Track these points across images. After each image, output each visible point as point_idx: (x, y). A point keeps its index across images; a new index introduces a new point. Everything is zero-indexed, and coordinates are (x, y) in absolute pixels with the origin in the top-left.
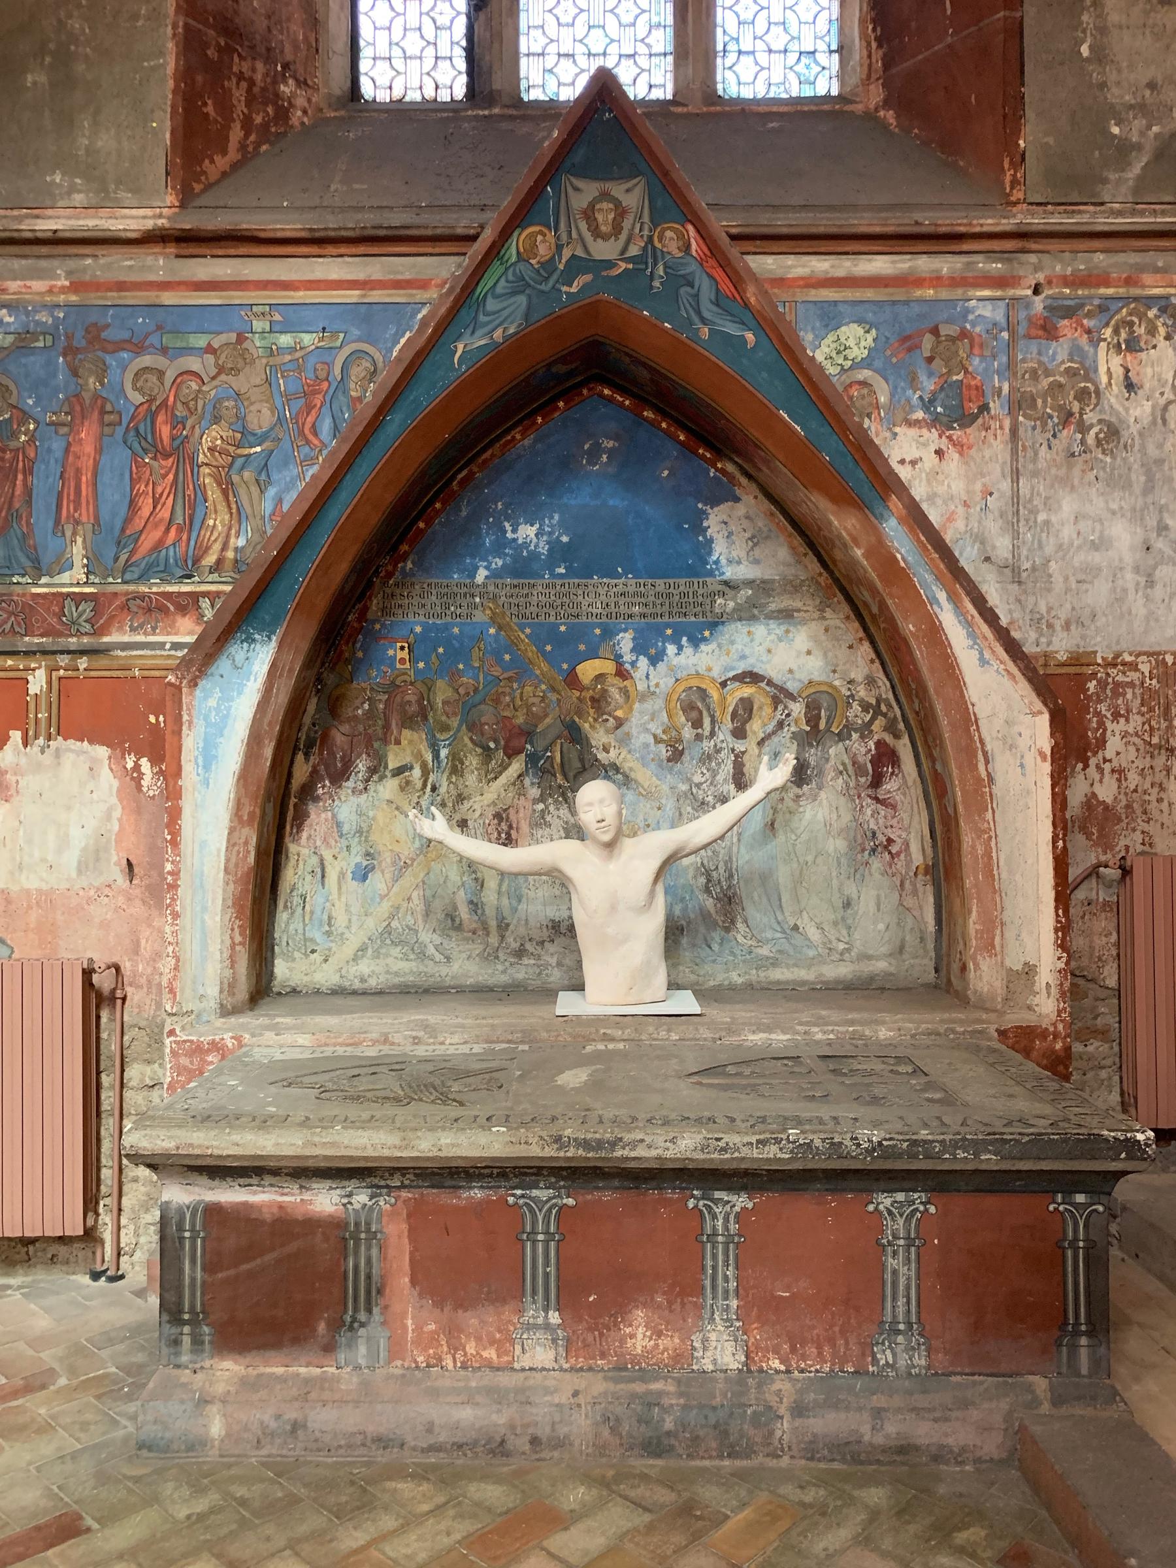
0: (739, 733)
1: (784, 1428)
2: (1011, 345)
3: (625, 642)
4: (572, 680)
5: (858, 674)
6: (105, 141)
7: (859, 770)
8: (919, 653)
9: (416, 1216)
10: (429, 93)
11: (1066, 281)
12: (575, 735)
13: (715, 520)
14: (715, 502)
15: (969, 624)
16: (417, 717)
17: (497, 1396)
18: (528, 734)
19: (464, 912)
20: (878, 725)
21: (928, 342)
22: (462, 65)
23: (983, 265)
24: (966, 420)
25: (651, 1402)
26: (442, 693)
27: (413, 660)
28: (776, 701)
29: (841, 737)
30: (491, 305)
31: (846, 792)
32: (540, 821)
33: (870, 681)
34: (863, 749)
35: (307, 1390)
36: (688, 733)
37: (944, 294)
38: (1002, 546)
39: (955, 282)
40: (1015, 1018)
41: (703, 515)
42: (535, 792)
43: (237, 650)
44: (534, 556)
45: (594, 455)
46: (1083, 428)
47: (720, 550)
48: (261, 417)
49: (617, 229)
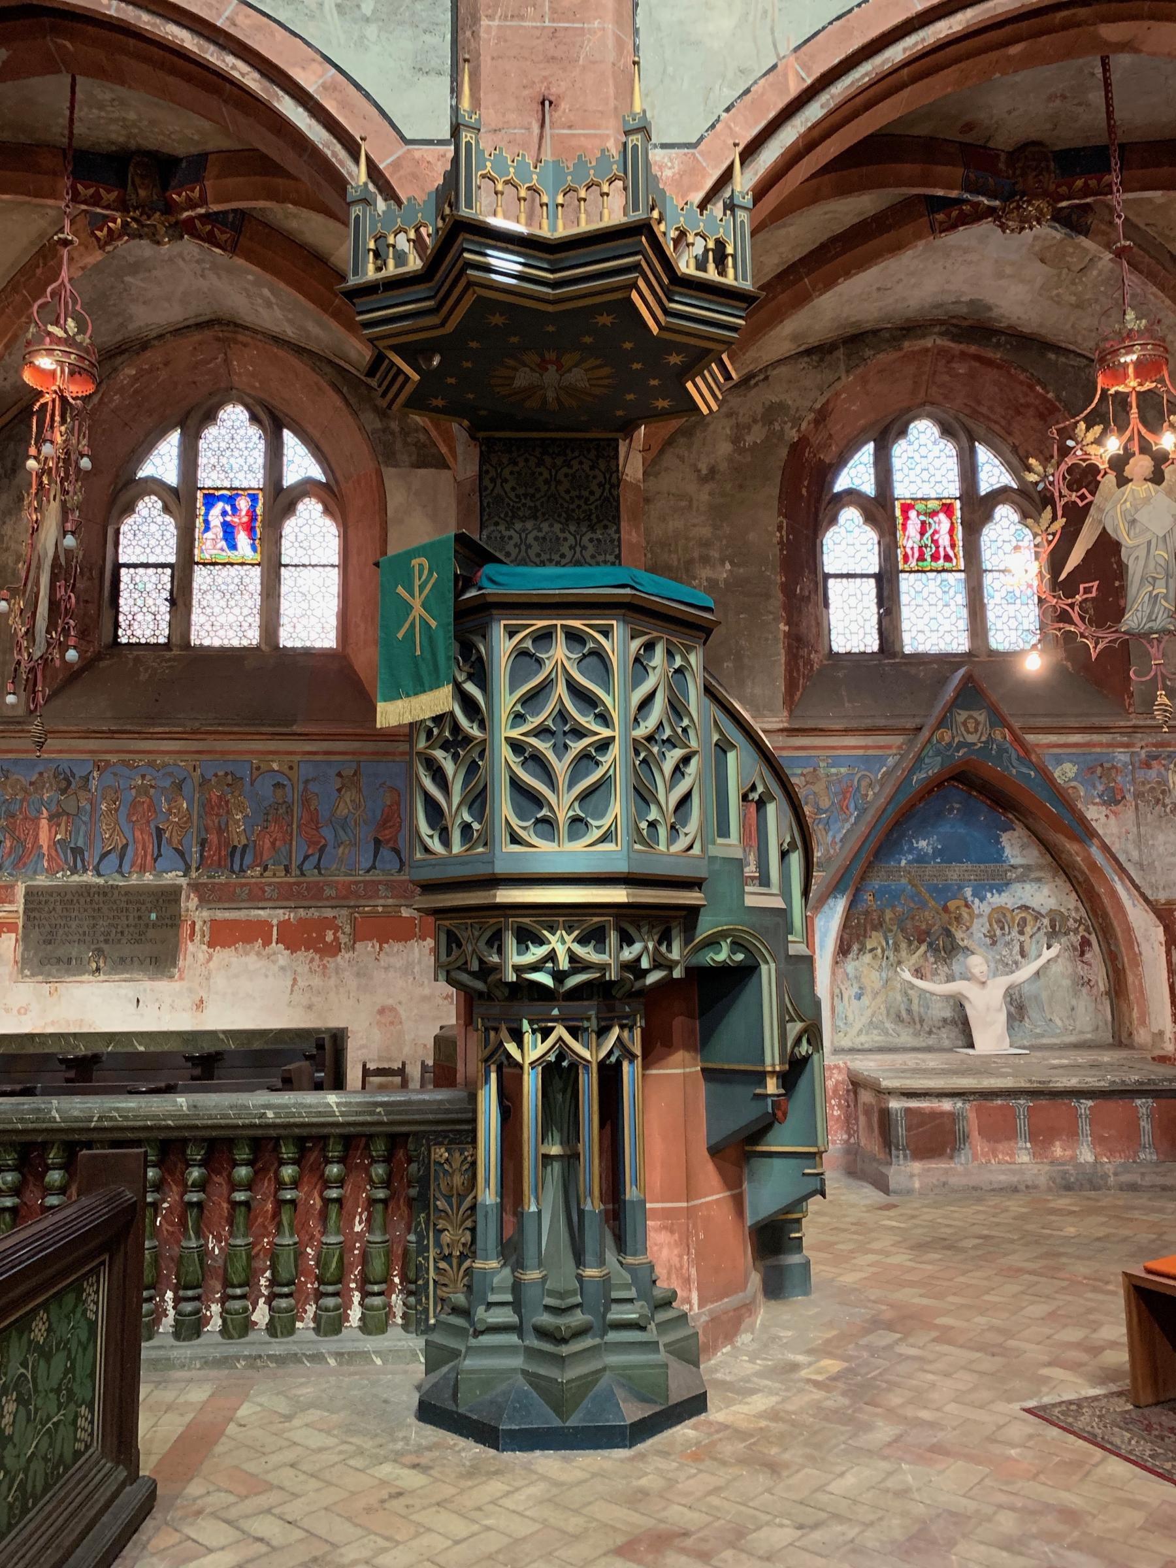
0: (1021, 933)
1: (1112, 1180)
2: (1133, 772)
3: (968, 892)
4: (946, 909)
5: (1071, 907)
6: (758, 691)
7: (1075, 949)
8: (1106, 900)
9: (979, 1110)
10: (862, 649)
11: (1155, 745)
12: (949, 934)
13: (1005, 838)
14: (1005, 831)
15: (1127, 890)
16: (878, 926)
17: (1014, 1172)
18: (928, 933)
19: (904, 1014)
20: (1082, 928)
21: (1099, 770)
22: (876, 636)
23: (1119, 738)
24: (1117, 803)
25: (1066, 1172)
26: (888, 915)
27: (875, 900)
28: (1036, 918)
29: (1066, 934)
30: (927, 760)
31: (1070, 959)
32: (935, 973)
33: (1077, 909)
34: (1075, 939)
35: (946, 1171)
36: (998, 932)
37: (1104, 750)
38: (1135, 855)
39: (1109, 745)
40: (1158, 1052)
41: (999, 836)
42: (932, 960)
43: (831, 902)
44: (926, 854)
45: (951, 810)
46: (1165, 806)
47: (1008, 852)
48: (825, 803)
49: (976, 730)
